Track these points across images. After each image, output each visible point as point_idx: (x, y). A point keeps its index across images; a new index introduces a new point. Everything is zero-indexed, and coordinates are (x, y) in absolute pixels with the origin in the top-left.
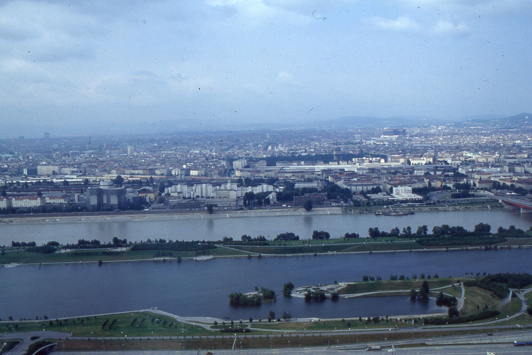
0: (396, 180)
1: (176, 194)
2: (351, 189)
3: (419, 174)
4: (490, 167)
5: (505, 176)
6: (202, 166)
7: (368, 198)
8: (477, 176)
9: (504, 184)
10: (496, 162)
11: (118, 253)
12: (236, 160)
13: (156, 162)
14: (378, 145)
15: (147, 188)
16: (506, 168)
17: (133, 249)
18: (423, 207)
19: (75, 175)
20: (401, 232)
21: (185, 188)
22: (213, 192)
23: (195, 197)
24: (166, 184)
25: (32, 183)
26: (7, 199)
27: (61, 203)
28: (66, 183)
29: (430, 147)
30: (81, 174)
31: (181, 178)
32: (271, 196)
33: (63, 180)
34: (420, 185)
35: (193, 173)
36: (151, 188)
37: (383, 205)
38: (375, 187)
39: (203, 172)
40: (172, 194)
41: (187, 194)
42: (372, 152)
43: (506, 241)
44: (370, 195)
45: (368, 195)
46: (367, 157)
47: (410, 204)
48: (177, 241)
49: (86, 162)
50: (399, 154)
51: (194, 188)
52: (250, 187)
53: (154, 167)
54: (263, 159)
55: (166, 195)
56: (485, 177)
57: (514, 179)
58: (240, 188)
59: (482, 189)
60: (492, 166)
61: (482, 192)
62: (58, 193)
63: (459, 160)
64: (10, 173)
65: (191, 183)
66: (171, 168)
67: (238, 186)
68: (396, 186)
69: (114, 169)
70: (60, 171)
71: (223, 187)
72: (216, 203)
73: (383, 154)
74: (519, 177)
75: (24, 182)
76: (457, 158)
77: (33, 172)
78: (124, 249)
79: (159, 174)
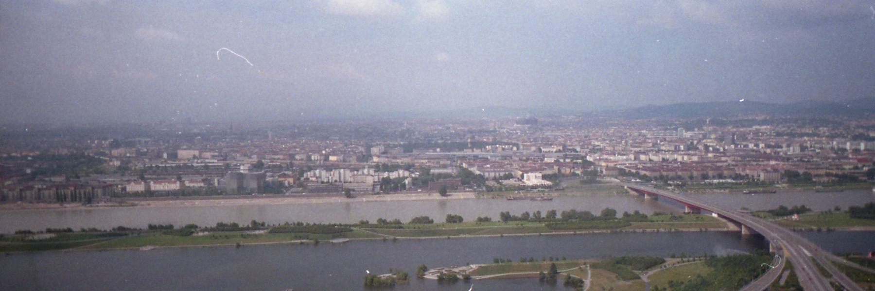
0: (526, 167)
1: (314, 179)
2: (484, 175)
3: (549, 161)
4: (616, 155)
5: (631, 164)
6: (341, 151)
7: (501, 184)
8: (604, 164)
9: (630, 171)
10: (622, 150)
11: (256, 236)
12: (374, 146)
13: (295, 147)
14: (511, 133)
15: (286, 172)
16: (632, 157)
17: (271, 232)
18: (553, 192)
19: (216, 159)
20: (531, 215)
21: (324, 173)
22: (350, 177)
23: (333, 181)
24: (305, 169)
25: (172, 167)
26: (145, 182)
27: (201, 187)
28: (206, 167)
29: (560, 136)
30: (222, 158)
31: (320, 163)
32: (407, 181)
33: (203, 164)
34: (549, 172)
35: (332, 158)
36: (290, 173)
37: (515, 190)
38: (507, 173)
39: (341, 158)
40: (311, 179)
41: (326, 179)
42: (505, 140)
43: (630, 225)
44: (503, 181)
45: (500, 181)
46: (499, 145)
47: (540, 189)
48: (315, 224)
49: (227, 147)
50: (531, 142)
51: (332, 173)
52: (387, 173)
53: (294, 153)
54: (400, 145)
55: (305, 179)
56: (611, 165)
57: (639, 167)
58: (377, 174)
59: (608, 176)
60: (619, 154)
61: (608, 179)
62: (200, 178)
63: (588, 148)
64: (150, 157)
65: (329, 168)
66: (310, 154)
67: (375, 171)
68: (527, 172)
69: (254, 154)
70: (200, 155)
71: (360, 172)
72: (353, 188)
73: (516, 142)
74: (643, 165)
75: (164, 165)
76: (586, 146)
77: (173, 156)
78: (262, 232)
79: (298, 159)
